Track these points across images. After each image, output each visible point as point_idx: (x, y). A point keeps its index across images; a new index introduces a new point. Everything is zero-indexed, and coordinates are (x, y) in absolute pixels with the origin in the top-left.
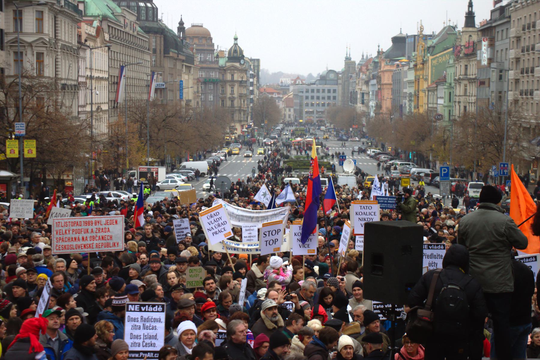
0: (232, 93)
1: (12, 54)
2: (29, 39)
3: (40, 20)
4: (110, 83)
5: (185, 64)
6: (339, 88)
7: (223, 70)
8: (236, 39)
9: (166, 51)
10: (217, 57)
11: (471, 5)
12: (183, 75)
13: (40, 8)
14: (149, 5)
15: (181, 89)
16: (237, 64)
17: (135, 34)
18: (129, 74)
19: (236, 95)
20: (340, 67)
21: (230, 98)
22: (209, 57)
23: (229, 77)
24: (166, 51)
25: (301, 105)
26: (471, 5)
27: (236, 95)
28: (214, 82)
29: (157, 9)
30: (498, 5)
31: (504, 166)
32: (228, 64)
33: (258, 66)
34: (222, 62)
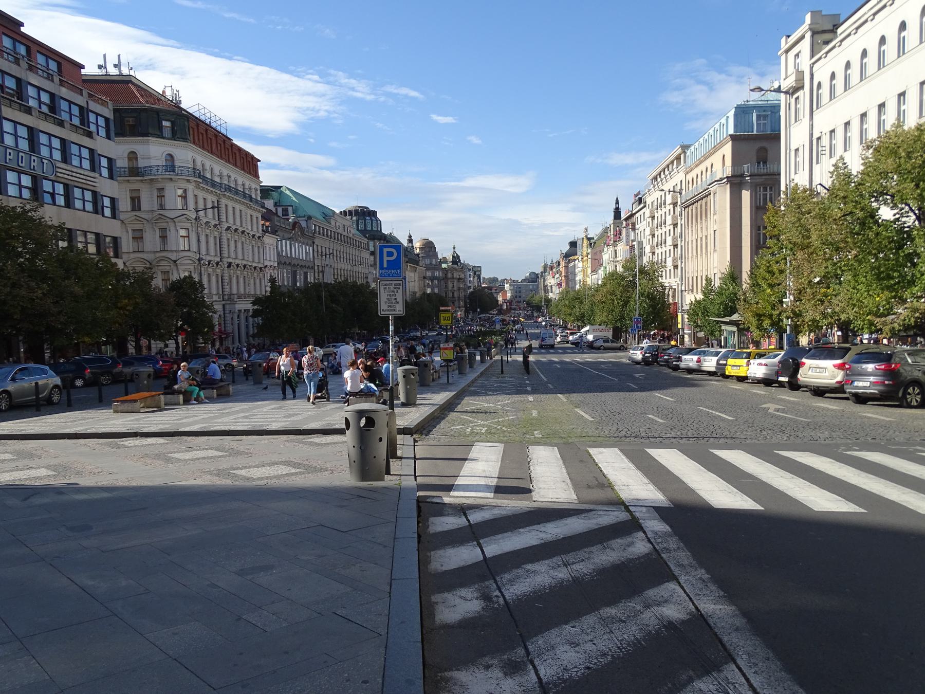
0: (453, 287)
1: (157, 231)
4: (317, 271)
5: (409, 264)
8: (454, 248)
11: (617, 202)
12: (407, 272)
14: (373, 218)
16: (456, 266)
17: (351, 235)
18: (343, 267)
20: (539, 270)
21: (451, 291)
22: (434, 261)
23: (450, 275)
26: (617, 202)
29: (381, 222)
30: (637, 198)
31: (637, 321)
33: (480, 271)
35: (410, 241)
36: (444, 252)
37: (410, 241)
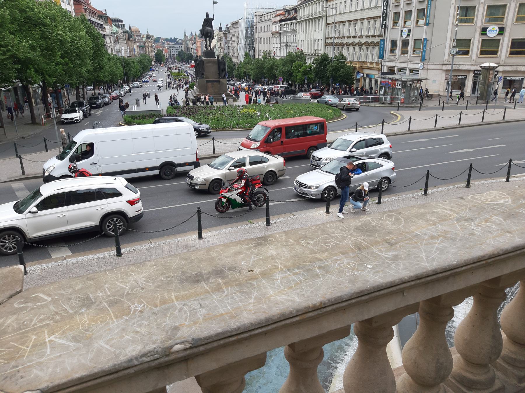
0: (149, 50)
2: (109, 45)
3: (110, 40)
6: (183, 46)
7: (145, 42)
9: (129, 39)
10: (142, 37)
11: (220, 25)
13: (110, 37)
15: (134, 51)
19: (150, 51)
23: (147, 45)
24: (129, 39)
25: (170, 52)
26: (220, 25)
27: (150, 51)
28: (142, 47)
32: (146, 40)
34: (144, 39)
35: (130, 29)
36: (144, 33)
37: (130, 29)
